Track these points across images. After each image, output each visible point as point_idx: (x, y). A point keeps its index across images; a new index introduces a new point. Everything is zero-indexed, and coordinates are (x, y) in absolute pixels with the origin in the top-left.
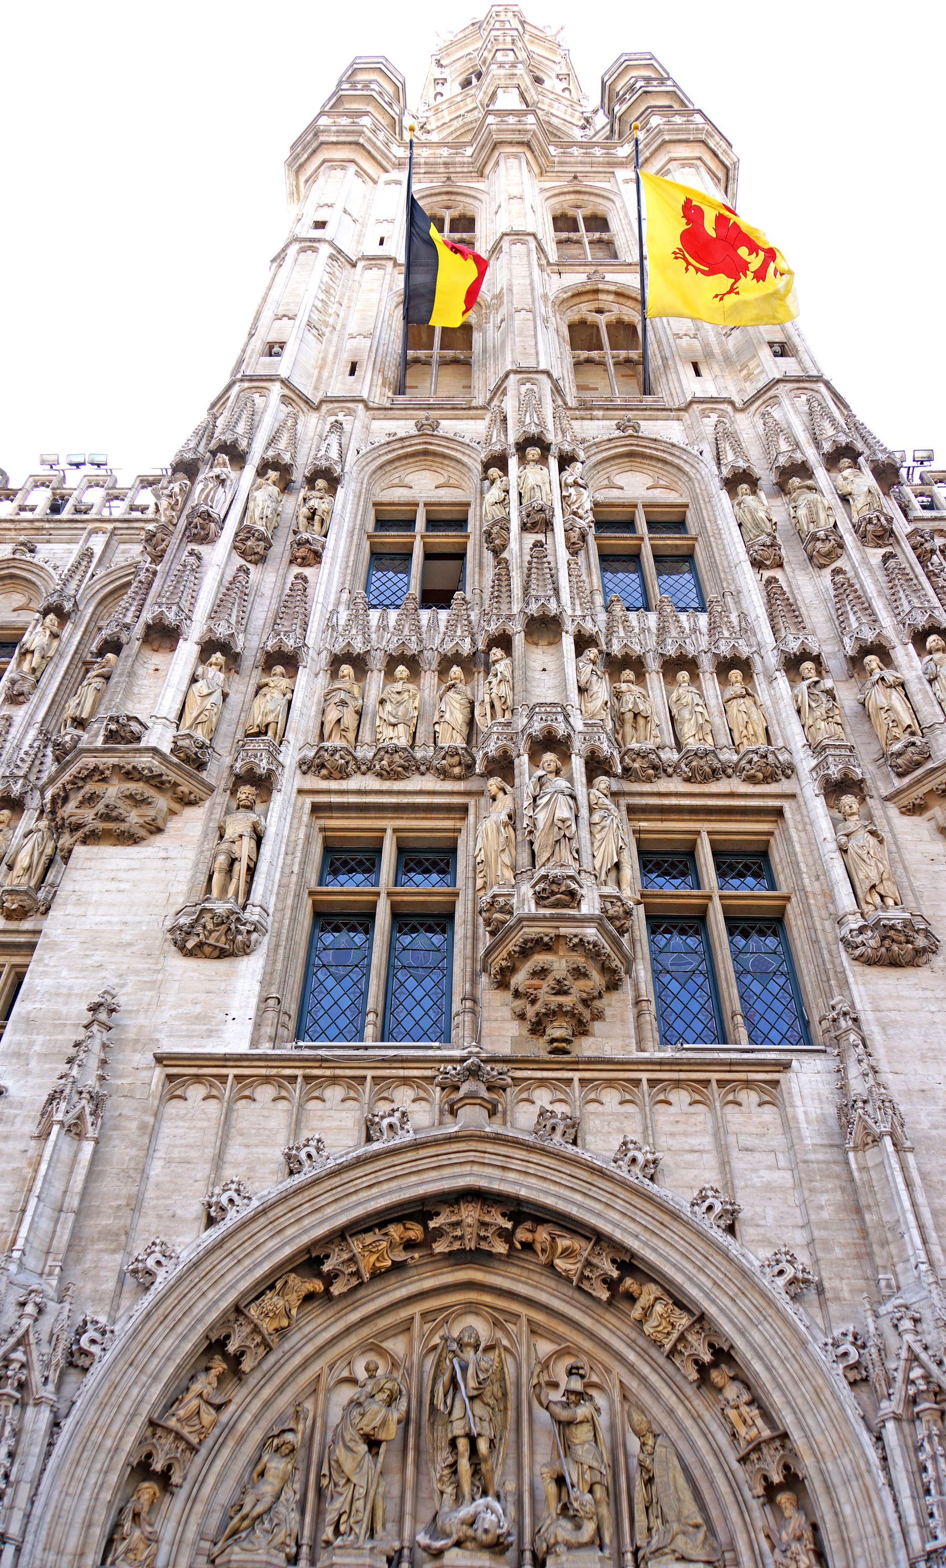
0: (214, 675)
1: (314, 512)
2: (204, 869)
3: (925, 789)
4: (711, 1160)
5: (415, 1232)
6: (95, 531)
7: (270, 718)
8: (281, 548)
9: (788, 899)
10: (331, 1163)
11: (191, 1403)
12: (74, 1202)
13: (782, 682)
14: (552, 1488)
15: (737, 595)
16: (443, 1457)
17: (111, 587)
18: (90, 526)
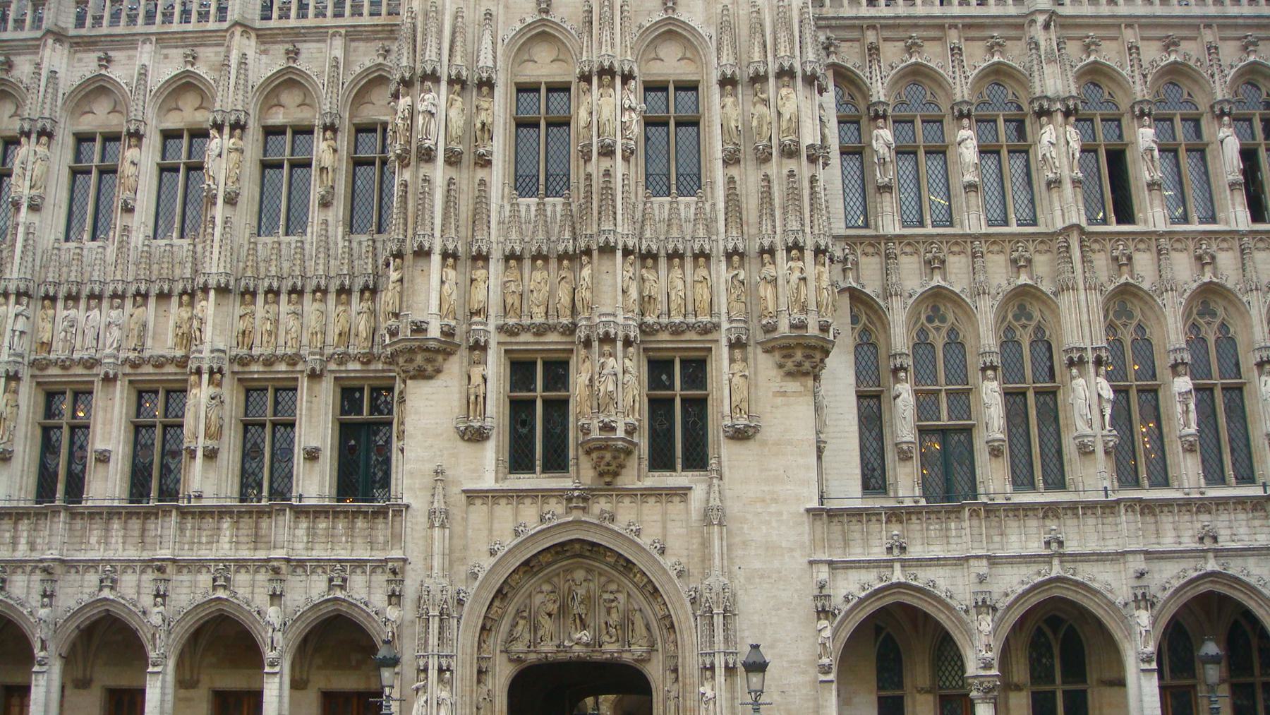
0: (451, 274)
1: (483, 125)
2: (464, 395)
3: (773, 344)
4: (659, 524)
5: (559, 549)
6: (334, 35)
7: (481, 306)
8: (467, 159)
9: (708, 395)
10: (530, 533)
11: (494, 609)
12: (447, 551)
13: (723, 265)
14: (604, 626)
15: (712, 183)
16: (572, 616)
17: (355, 91)
18: (331, 31)
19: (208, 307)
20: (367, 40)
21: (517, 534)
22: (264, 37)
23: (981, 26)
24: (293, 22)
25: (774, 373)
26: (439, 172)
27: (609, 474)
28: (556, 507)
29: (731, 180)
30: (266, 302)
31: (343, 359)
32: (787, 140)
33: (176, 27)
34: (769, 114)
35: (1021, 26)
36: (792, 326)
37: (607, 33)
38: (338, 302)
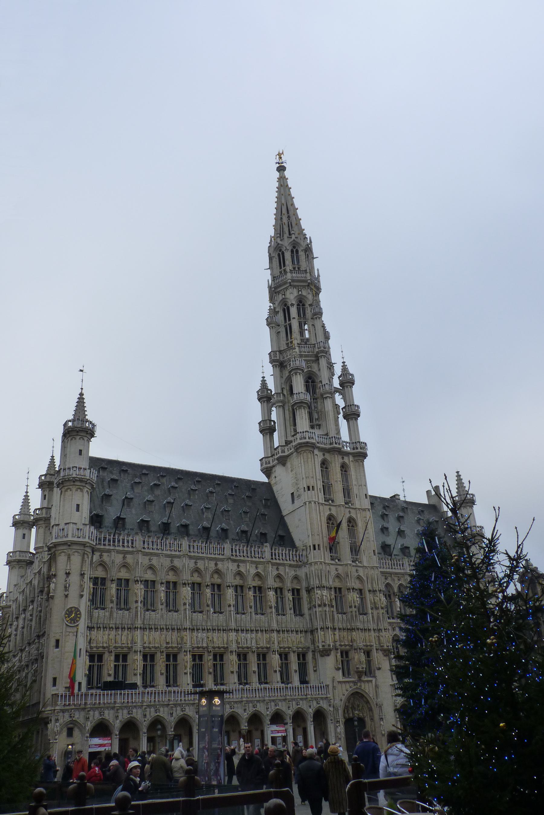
19: (275, 634)
20: (293, 567)
21: (347, 691)
22: (273, 564)
23: (398, 574)
24: (278, 561)
25: (382, 655)
26: (327, 609)
27: (360, 677)
28: (352, 684)
29: (372, 613)
30: (282, 633)
31: (300, 647)
32: (383, 606)
33: (254, 559)
34: (378, 599)
35: (403, 574)
36: (387, 646)
37: (352, 580)
38: (296, 634)
